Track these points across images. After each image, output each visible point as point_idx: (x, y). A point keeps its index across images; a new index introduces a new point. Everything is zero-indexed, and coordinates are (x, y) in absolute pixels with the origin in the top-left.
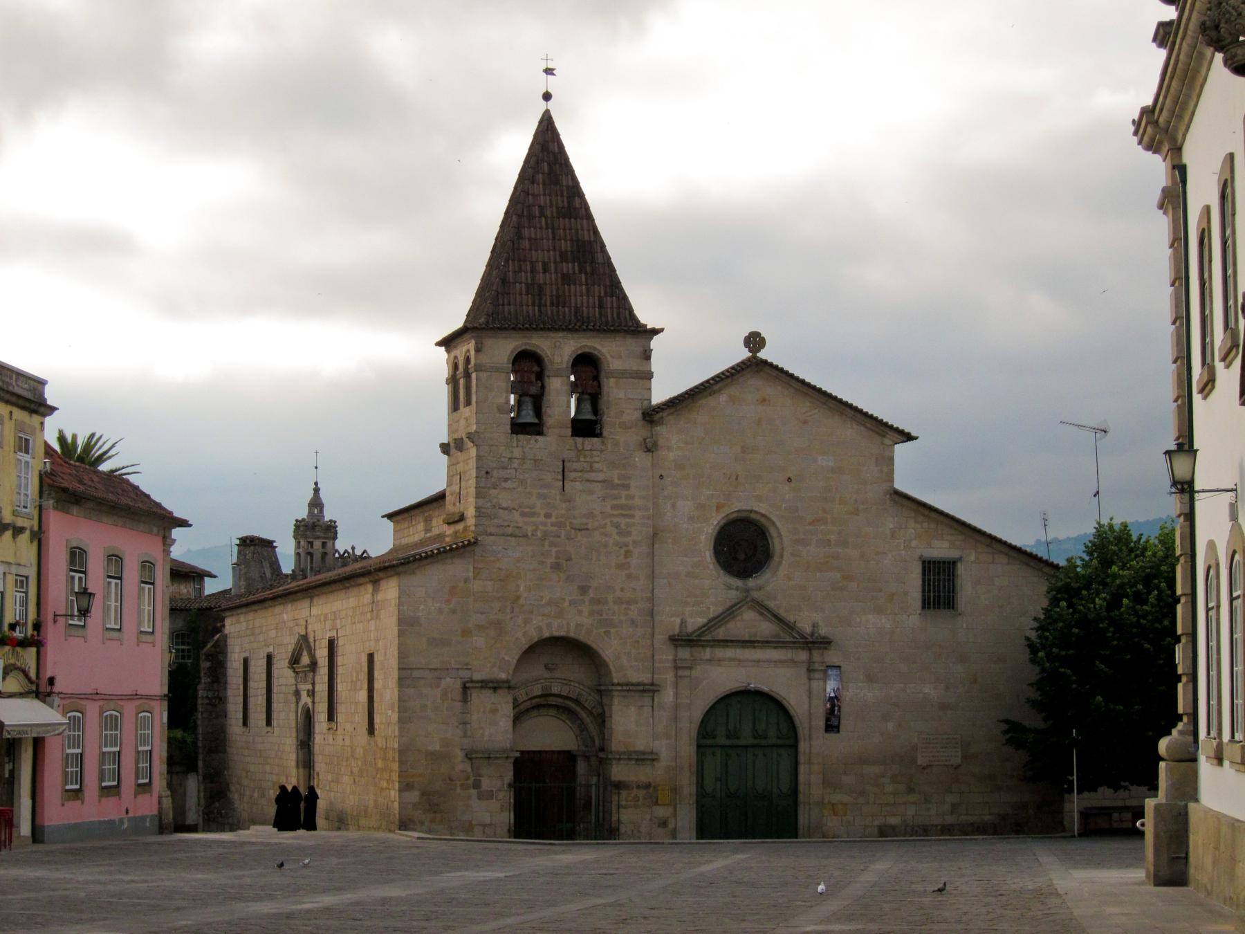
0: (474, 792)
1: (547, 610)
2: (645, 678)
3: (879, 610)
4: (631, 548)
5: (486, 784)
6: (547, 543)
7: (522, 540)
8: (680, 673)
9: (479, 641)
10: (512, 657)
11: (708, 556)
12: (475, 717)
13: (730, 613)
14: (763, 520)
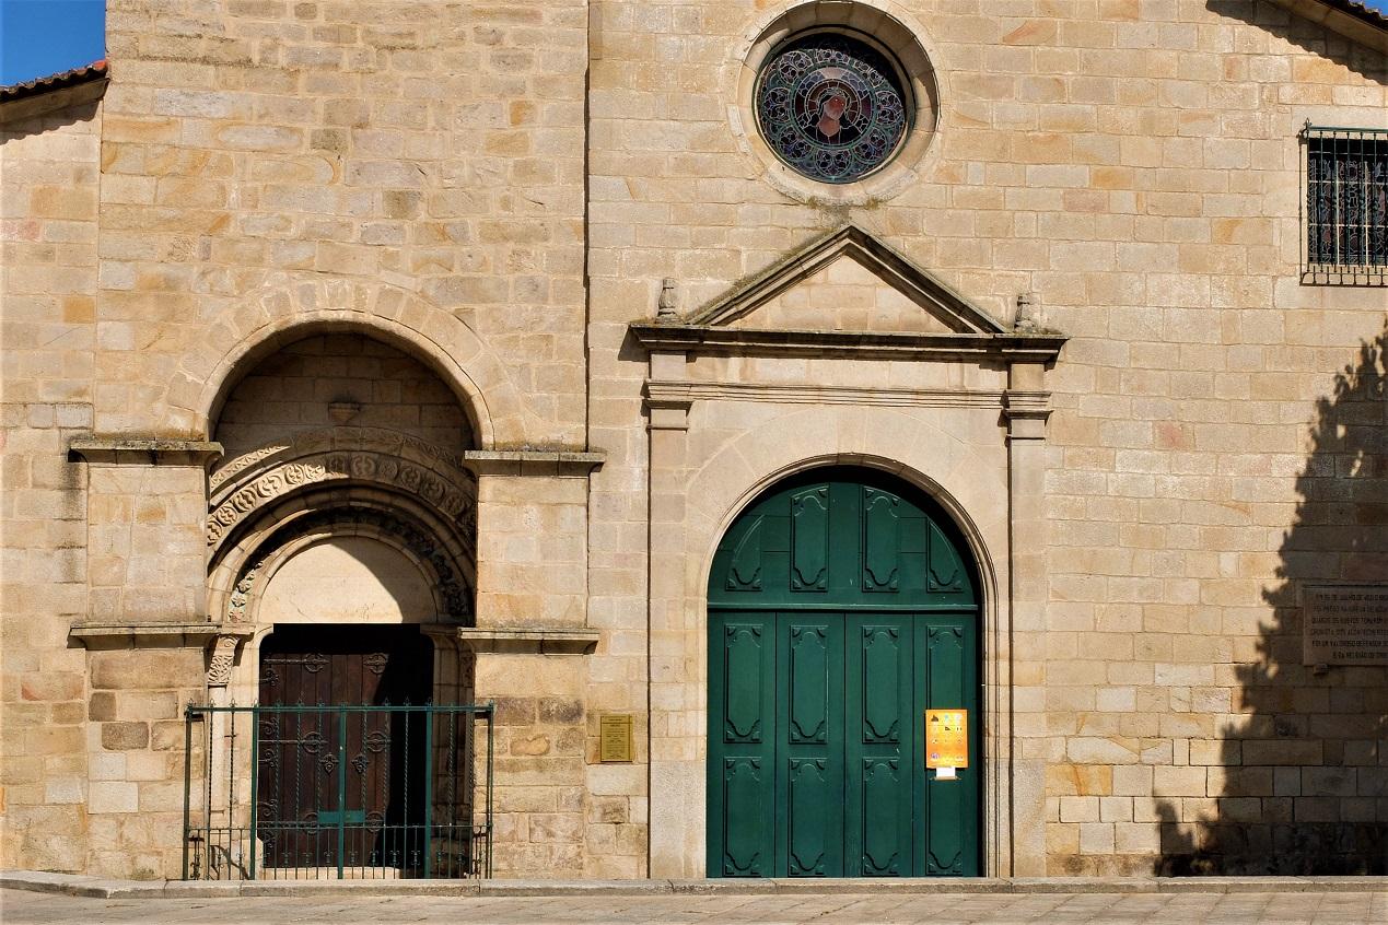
0: (93, 730)
1: (302, 253)
2: (568, 433)
3: (1192, 264)
4: (530, 97)
5: (128, 707)
6: (302, 79)
7: (233, 74)
8: (660, 417)
9: (115, 333)
10: (203, 380)
11: (740, 117)
12: (98, 532)
13: (792, 270)
14: (883, 34)
